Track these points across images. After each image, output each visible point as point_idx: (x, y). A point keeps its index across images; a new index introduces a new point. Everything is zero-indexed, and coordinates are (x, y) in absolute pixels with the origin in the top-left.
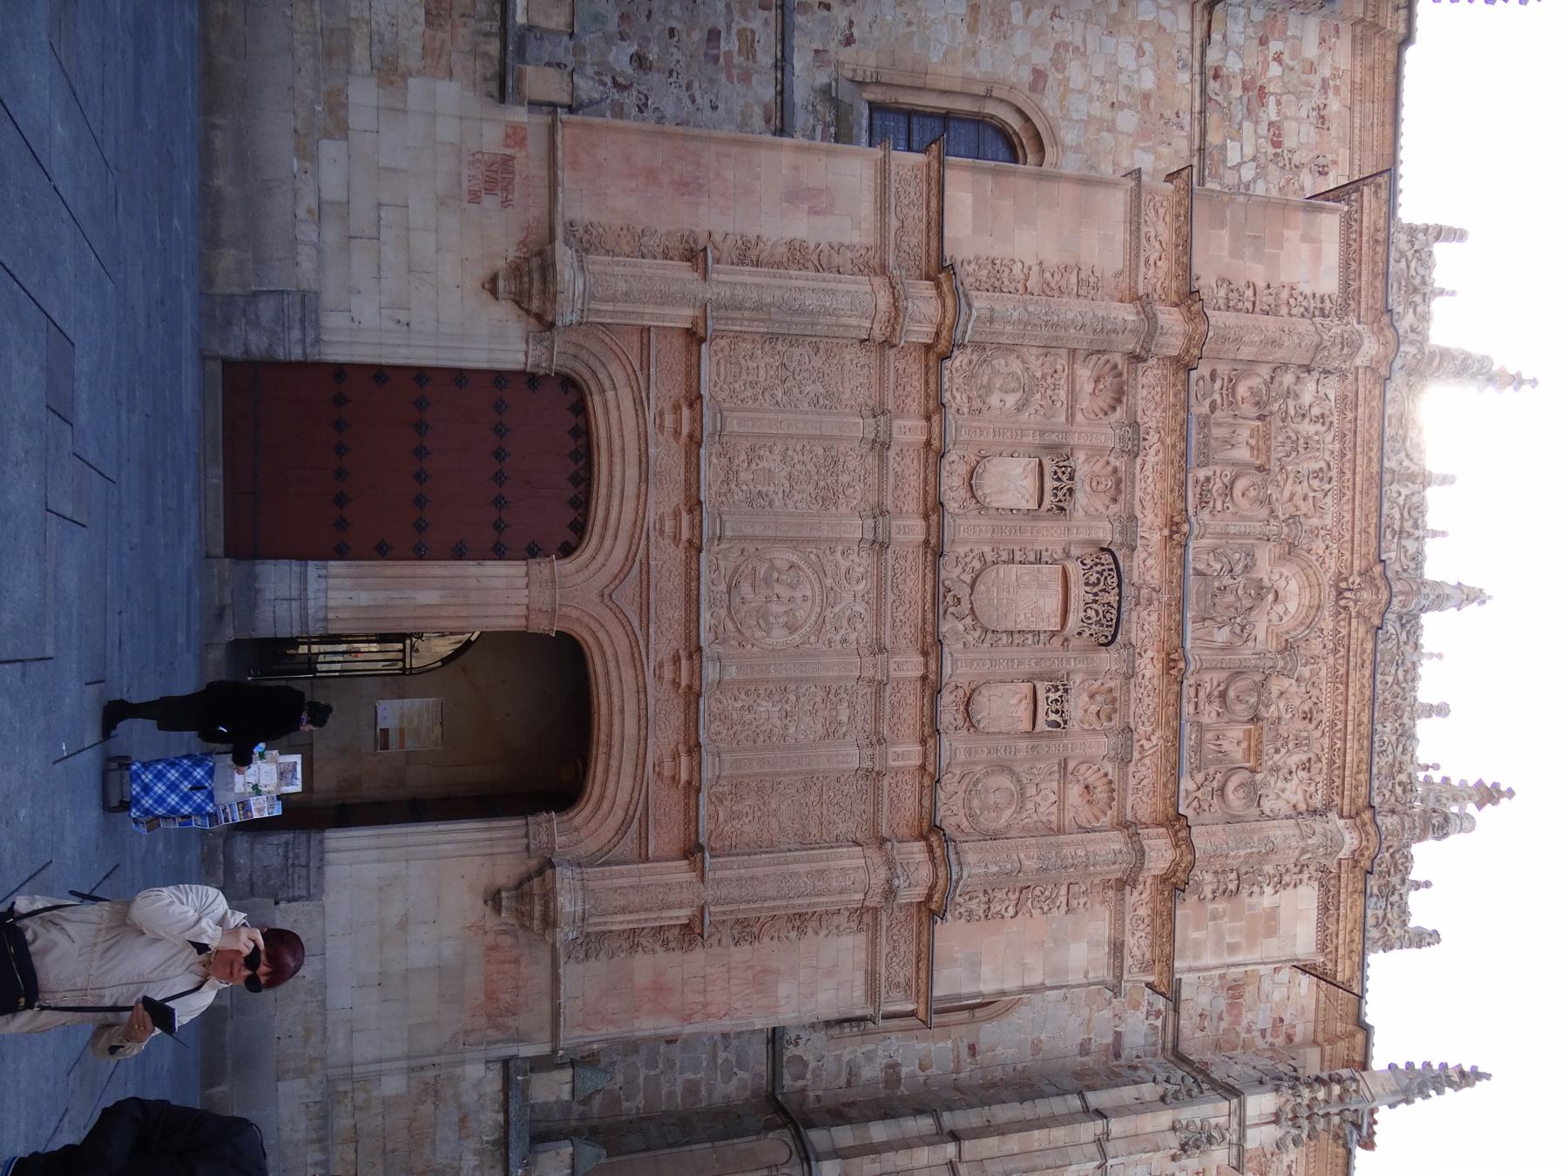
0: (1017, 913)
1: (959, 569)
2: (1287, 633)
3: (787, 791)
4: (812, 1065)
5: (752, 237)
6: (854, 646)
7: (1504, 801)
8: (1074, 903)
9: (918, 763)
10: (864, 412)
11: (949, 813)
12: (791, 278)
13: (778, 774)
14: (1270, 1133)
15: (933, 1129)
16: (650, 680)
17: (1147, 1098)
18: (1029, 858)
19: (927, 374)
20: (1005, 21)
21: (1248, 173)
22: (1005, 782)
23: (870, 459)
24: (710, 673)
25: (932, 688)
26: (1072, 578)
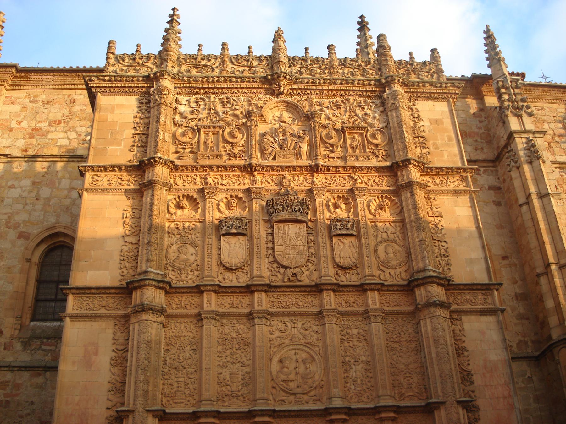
0: (445, 241)
1: (278, 274)
2: (300, 116)
3: (395, 359)
4: (520, 338)
5: (110, 386)
6: (319, 327)
7: (366, 19)
8: (437, 214)
9: (376, 292)
10: (200, 325)
11: (399, 277)
12: (131, 365)
13: (387, 364)
14: (526, 119)
15: (545, 277)
17: (518, 174)
18: (418, 237)
19: (179, 293)
21: (73, 135)
22: (381, 248)
23: (224, 321)
24: (337, 403)
25: (337, 288)
26: (280, 218)
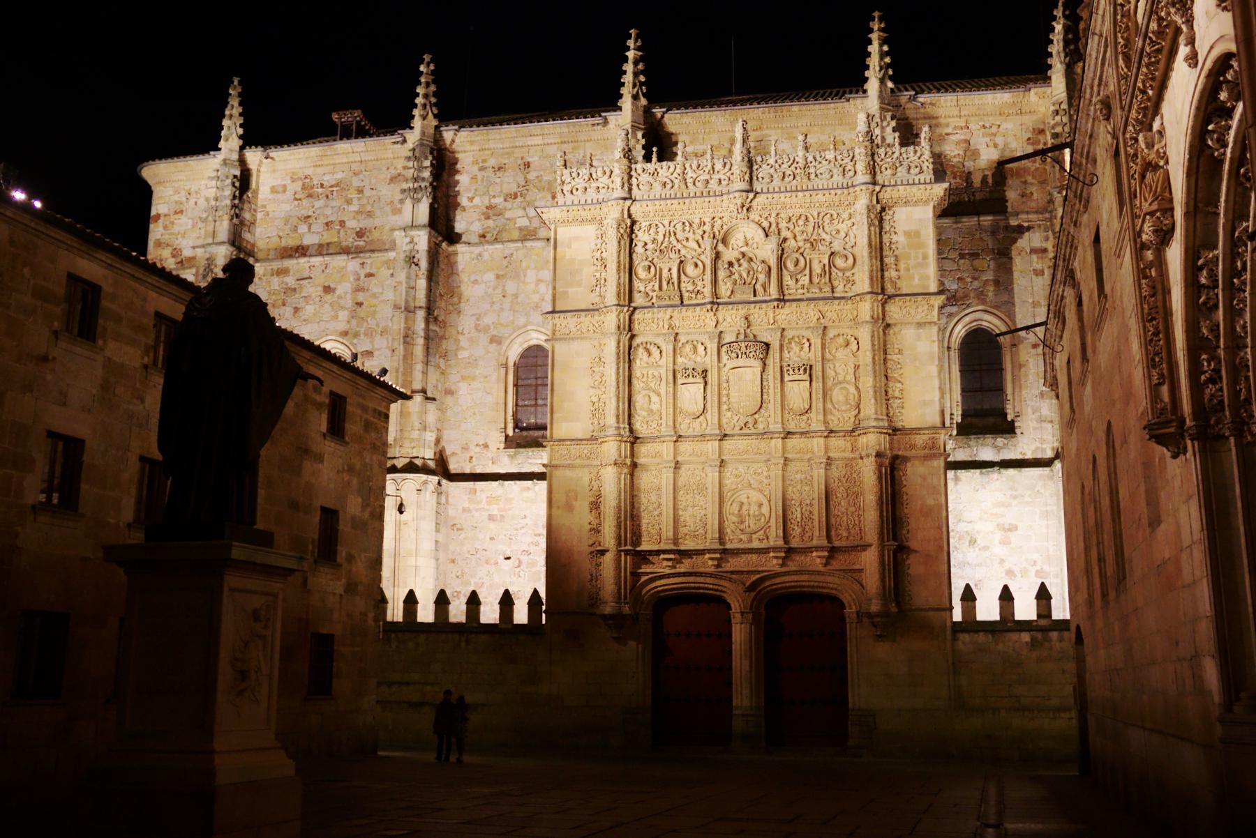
0: (900, 382)
4: (1038, 444)
16: (783, 569)
20: (468, 361)
